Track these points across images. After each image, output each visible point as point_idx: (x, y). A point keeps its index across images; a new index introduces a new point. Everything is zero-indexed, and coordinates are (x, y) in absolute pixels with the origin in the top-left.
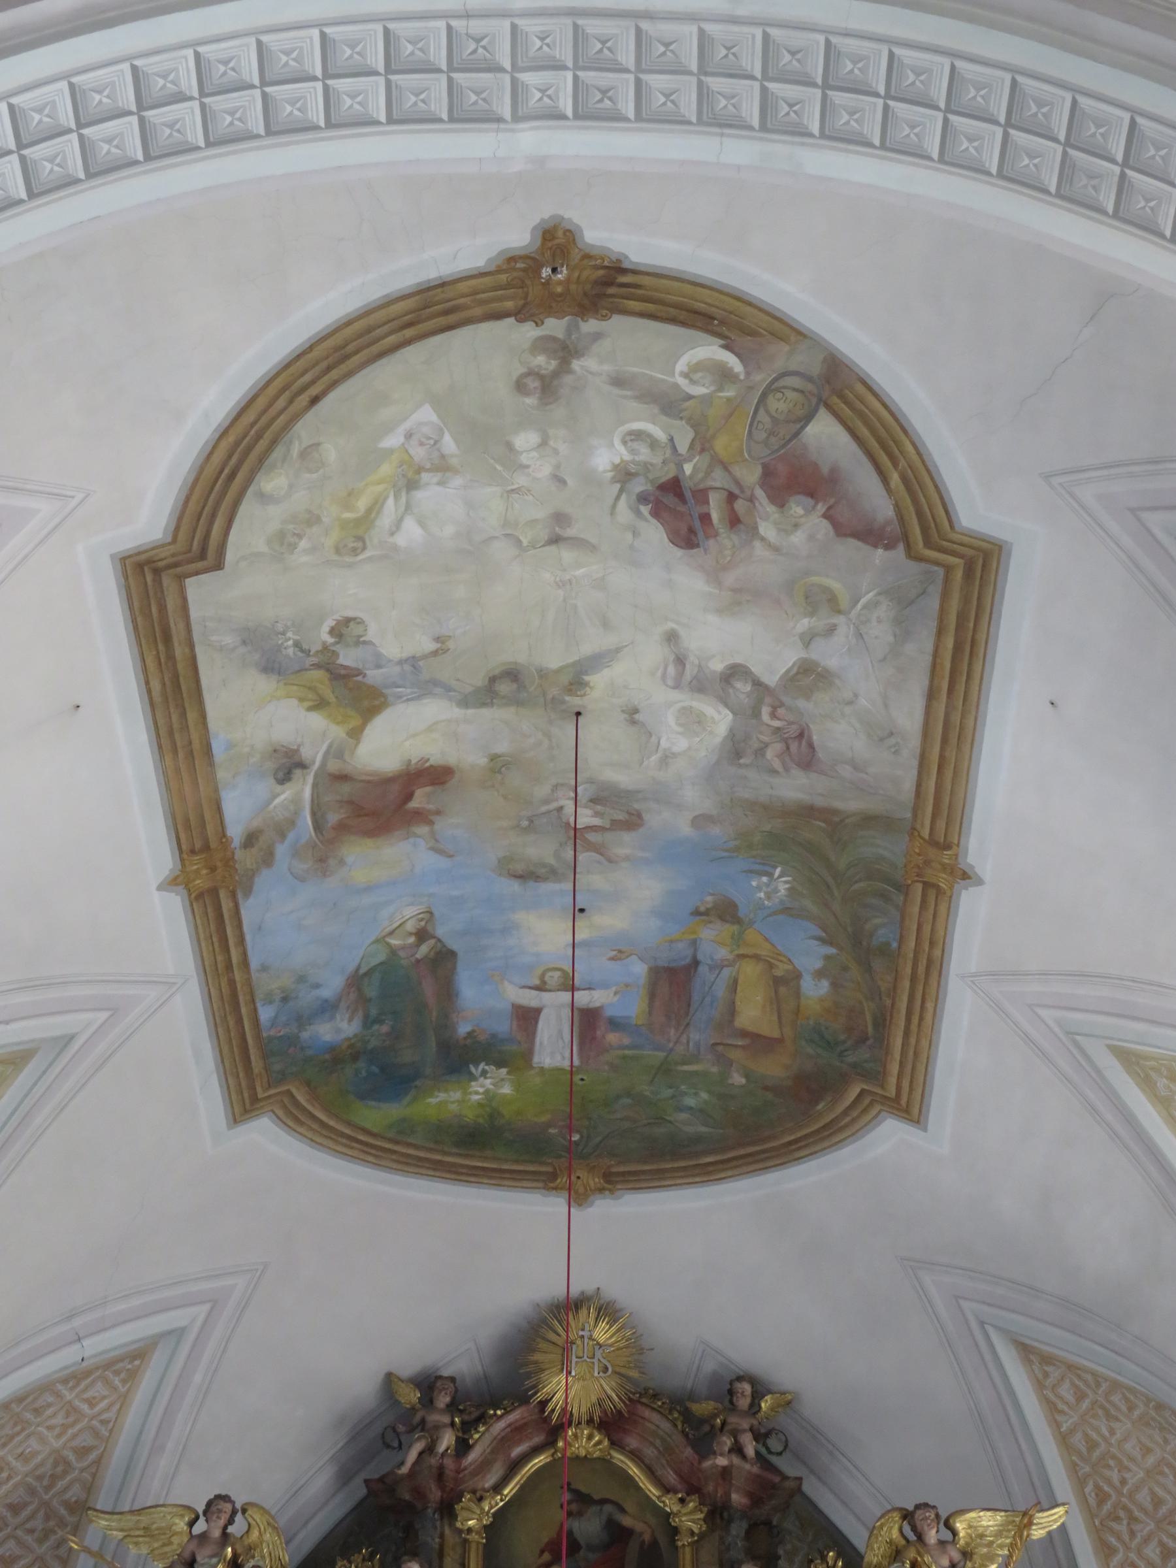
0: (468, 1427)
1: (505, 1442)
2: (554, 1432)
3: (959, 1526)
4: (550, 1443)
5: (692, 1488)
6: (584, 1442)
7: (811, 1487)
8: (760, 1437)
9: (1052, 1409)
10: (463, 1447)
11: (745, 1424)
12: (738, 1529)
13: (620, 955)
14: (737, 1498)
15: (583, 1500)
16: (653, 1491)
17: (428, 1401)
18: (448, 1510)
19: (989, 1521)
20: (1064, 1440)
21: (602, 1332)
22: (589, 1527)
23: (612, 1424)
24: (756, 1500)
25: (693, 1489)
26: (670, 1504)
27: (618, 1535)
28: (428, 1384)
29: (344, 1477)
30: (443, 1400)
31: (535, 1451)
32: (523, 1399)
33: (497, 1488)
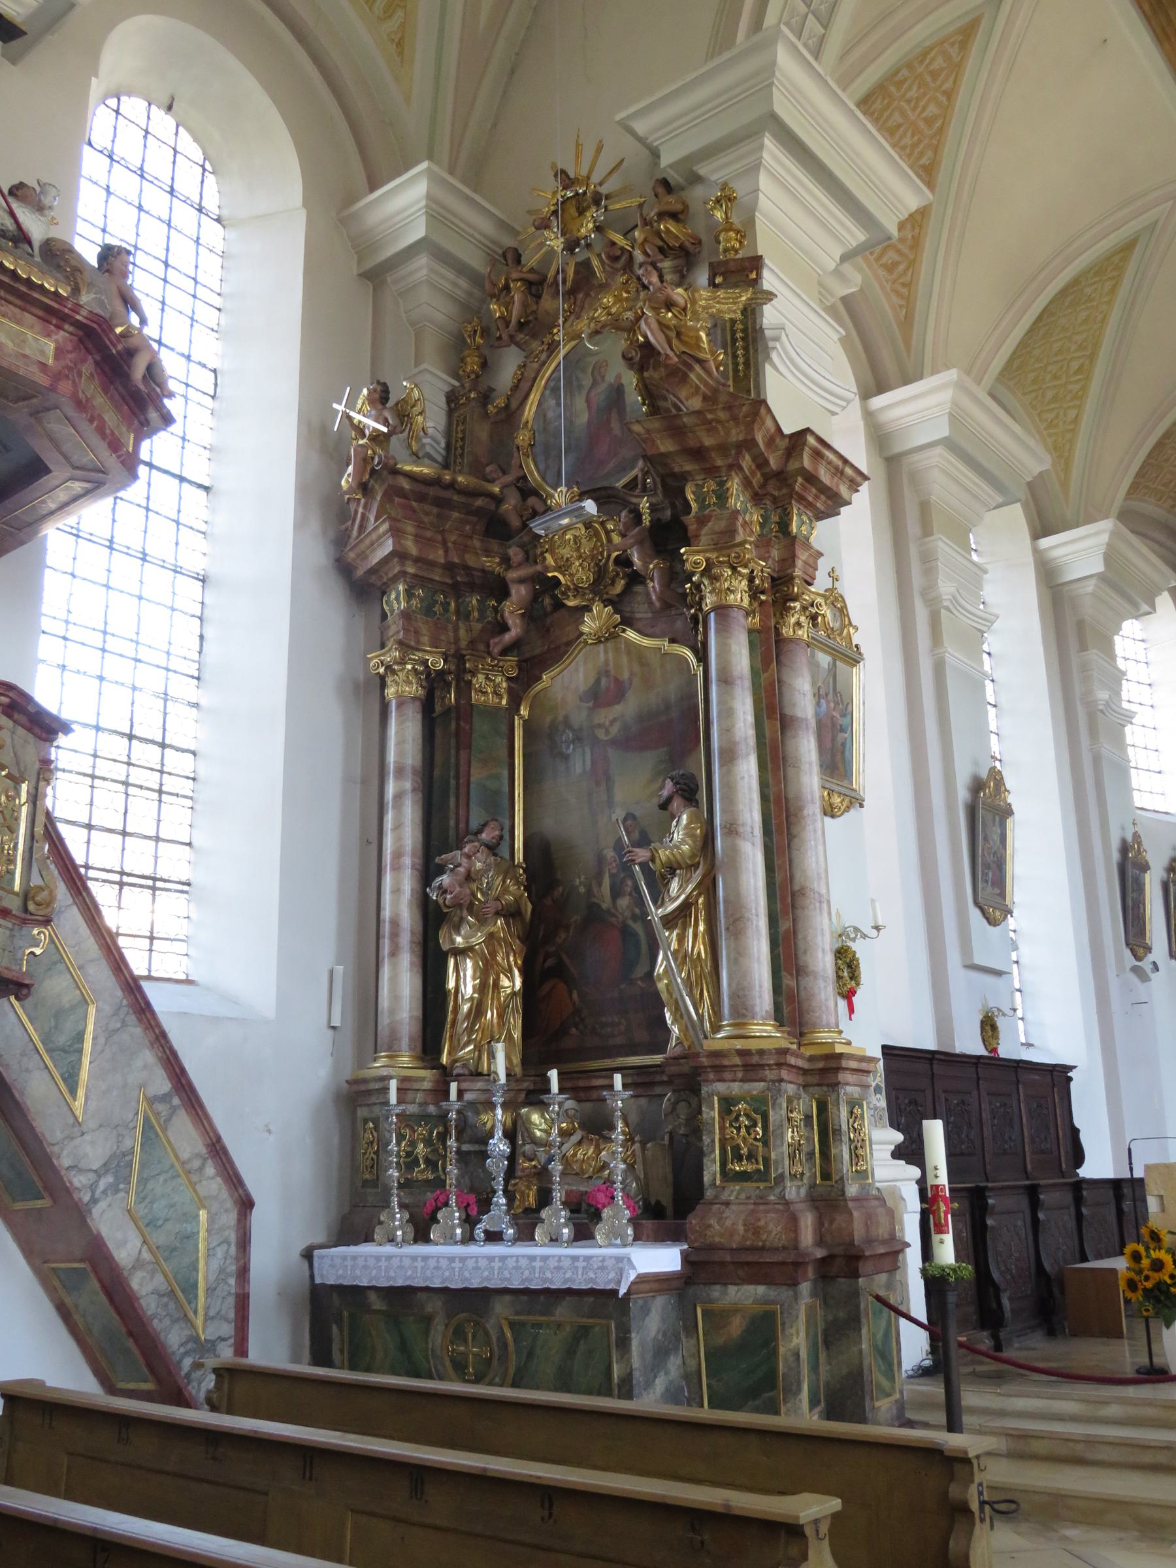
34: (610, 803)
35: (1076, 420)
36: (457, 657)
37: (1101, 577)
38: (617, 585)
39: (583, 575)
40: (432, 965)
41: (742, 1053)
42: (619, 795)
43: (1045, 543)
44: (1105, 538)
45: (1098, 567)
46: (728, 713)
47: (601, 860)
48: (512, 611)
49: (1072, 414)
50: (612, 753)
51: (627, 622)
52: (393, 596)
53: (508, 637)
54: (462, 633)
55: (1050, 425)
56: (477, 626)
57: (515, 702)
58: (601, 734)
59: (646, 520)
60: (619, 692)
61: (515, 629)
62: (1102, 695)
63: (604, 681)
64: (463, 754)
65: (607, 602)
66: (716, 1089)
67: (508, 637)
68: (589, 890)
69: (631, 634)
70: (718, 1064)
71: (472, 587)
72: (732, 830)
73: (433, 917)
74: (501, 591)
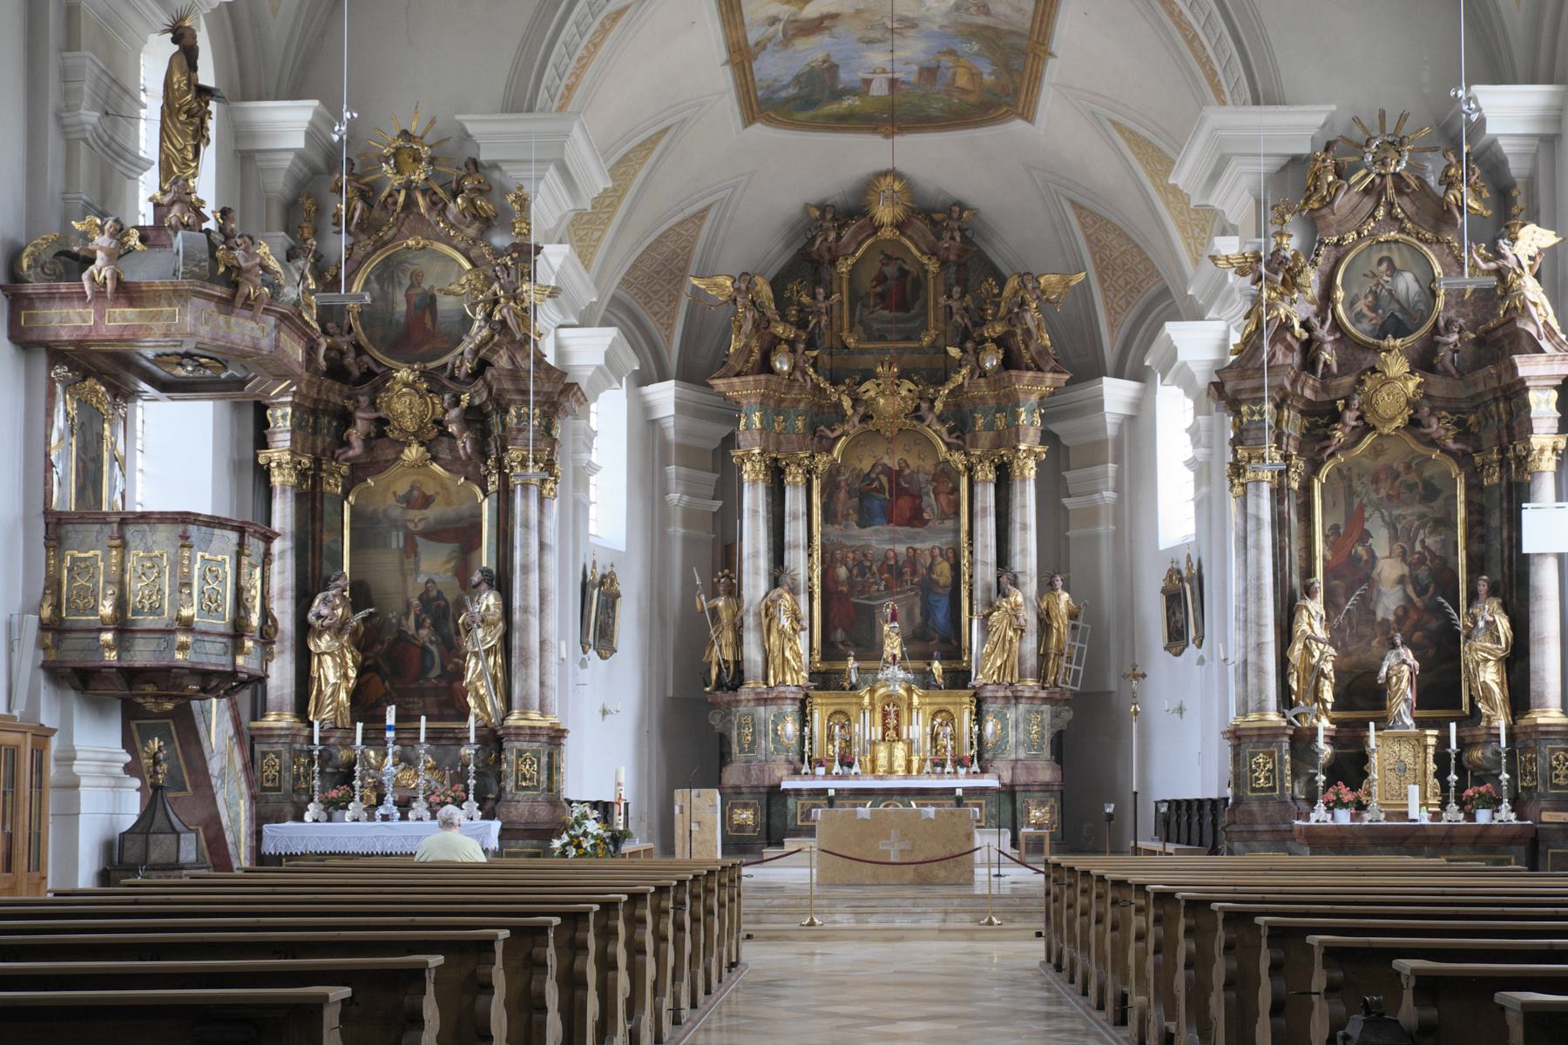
0: (840, 228)
1: (855, 234)
2: (877, 229)
3: (1042, 281)
4: (875, 233)
5: (933, 253)
6: (887, 233)
7: (983, 246)
8: (960, 229)
9: (1083, 226)
10: (839, 237)
11: (956, 225)
12: (953, 269)
13: (907, 63)
14: (952, 257)
15: (889, 258)
16: (917, 254)
17: (823, 217)
18: (833, 262)
19: (1054, 278)
20: (1088, 237)
21: (897, 186)
22: (890, 270)
23: (899, 226)
24: (959, 257)
25: (934, 254)
26: (925, 260)
27: (904, 273)
28: (823, 207)
29: (788, 245)
30: (829, 216)
31: (869, 236)
32: (864, 215)
33: (853, 254)
34: (417, 571)
35: (599, 239)
36: (317, 462)
37: (599, 368)
38: (435, 437)
39: (410, 424)
40: (304, 659)
41: (531, 728)
42: (424, 566)
43: (563, 332)
44: (609, 340)
45: (601, 361)
46: (525, 545)
47: (408, 605)
48: (356, 435)
49: (597, 234)
50: (419, 540)
51: (434, 459)
52: (279, 413)
53: (351, 453)
54: (319, 443)
55: (581, 240)
56: (328, 439)
57: (346, 495)
58: (411, 526)
59: (464, 404)
60: (427, 501)
61: (357, 448)
62: (585, 456)
63: (416, 493)
64: (318, 525)
65: (422, 444)
66: (512, 748)
67: (351, 453)
68: (399, 623)
69: (436, 467)
70: (518, 732)
71: (325, 412)
72: (525, 610)
73: (304, 629)
74: (346, 419)
